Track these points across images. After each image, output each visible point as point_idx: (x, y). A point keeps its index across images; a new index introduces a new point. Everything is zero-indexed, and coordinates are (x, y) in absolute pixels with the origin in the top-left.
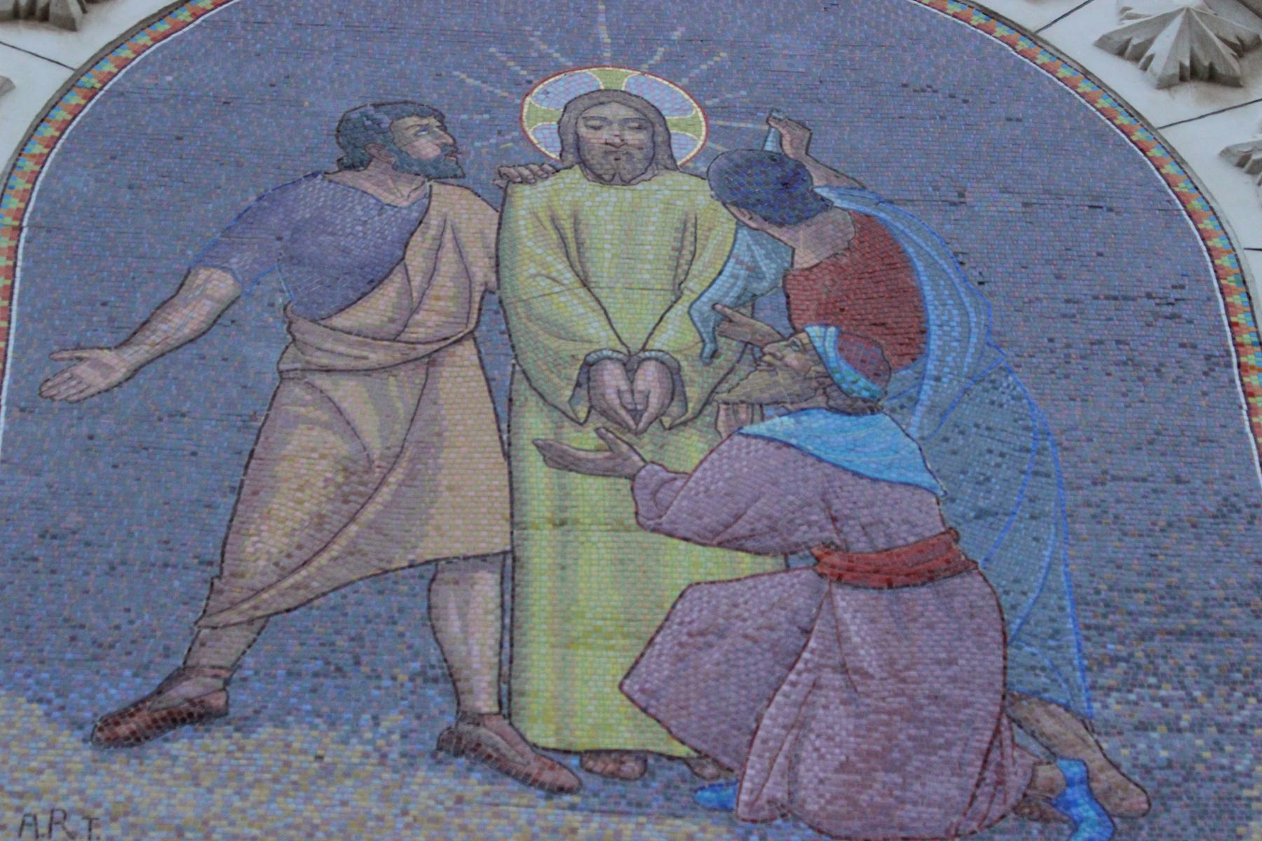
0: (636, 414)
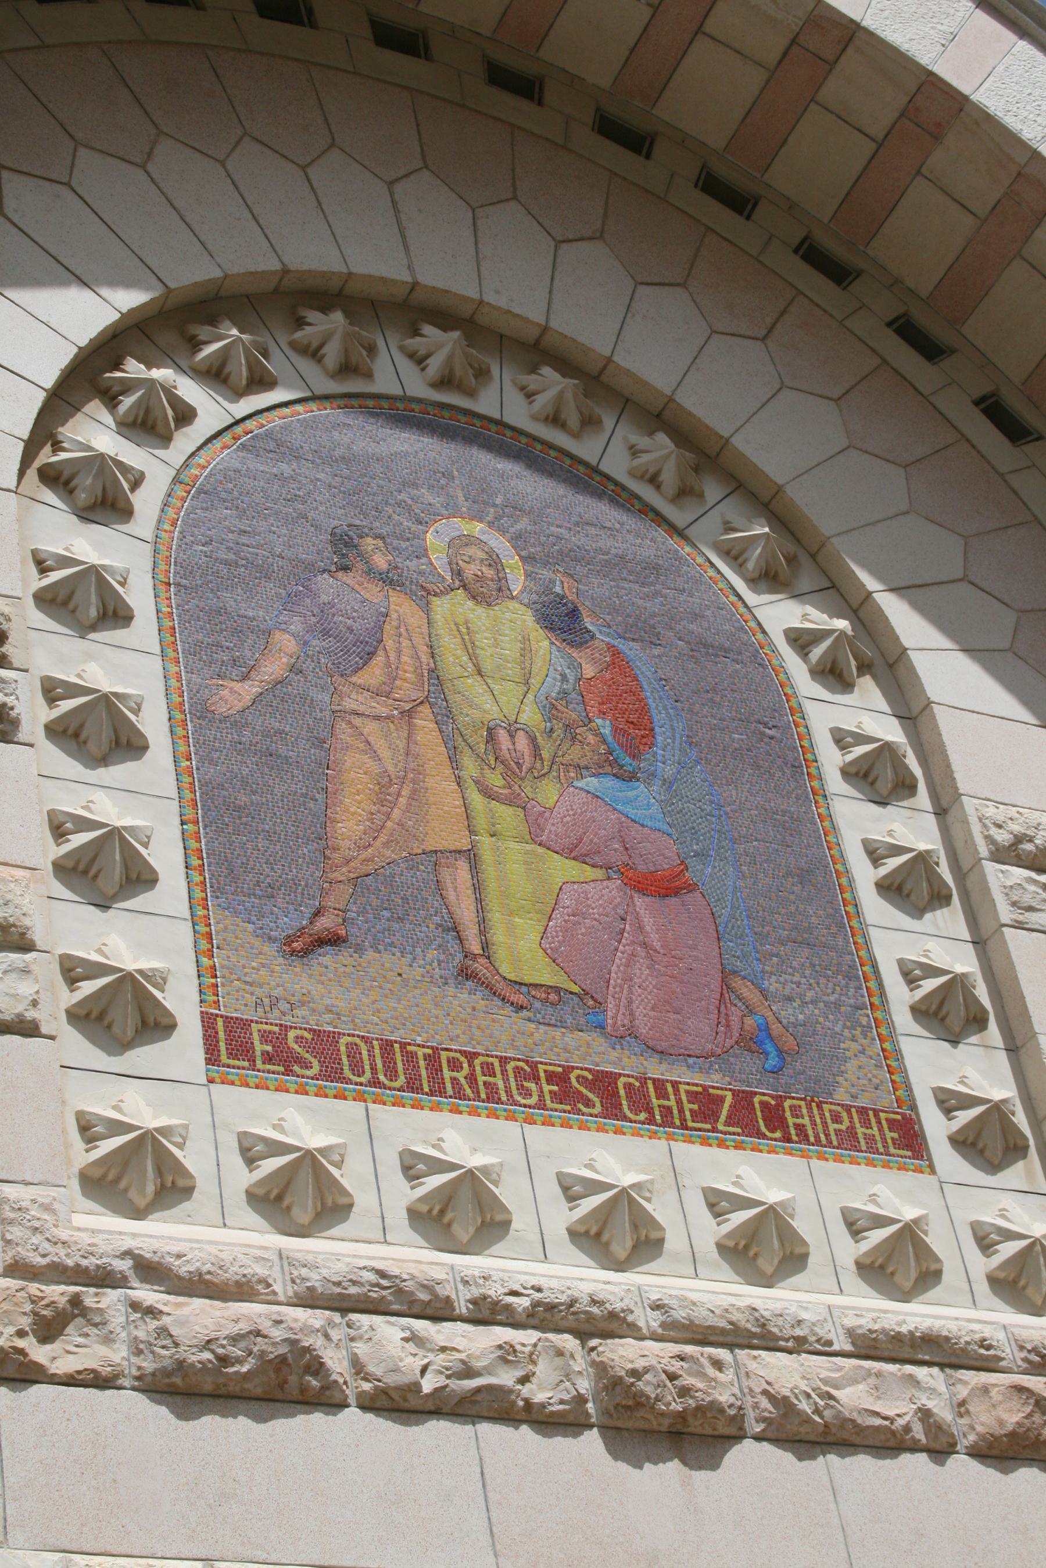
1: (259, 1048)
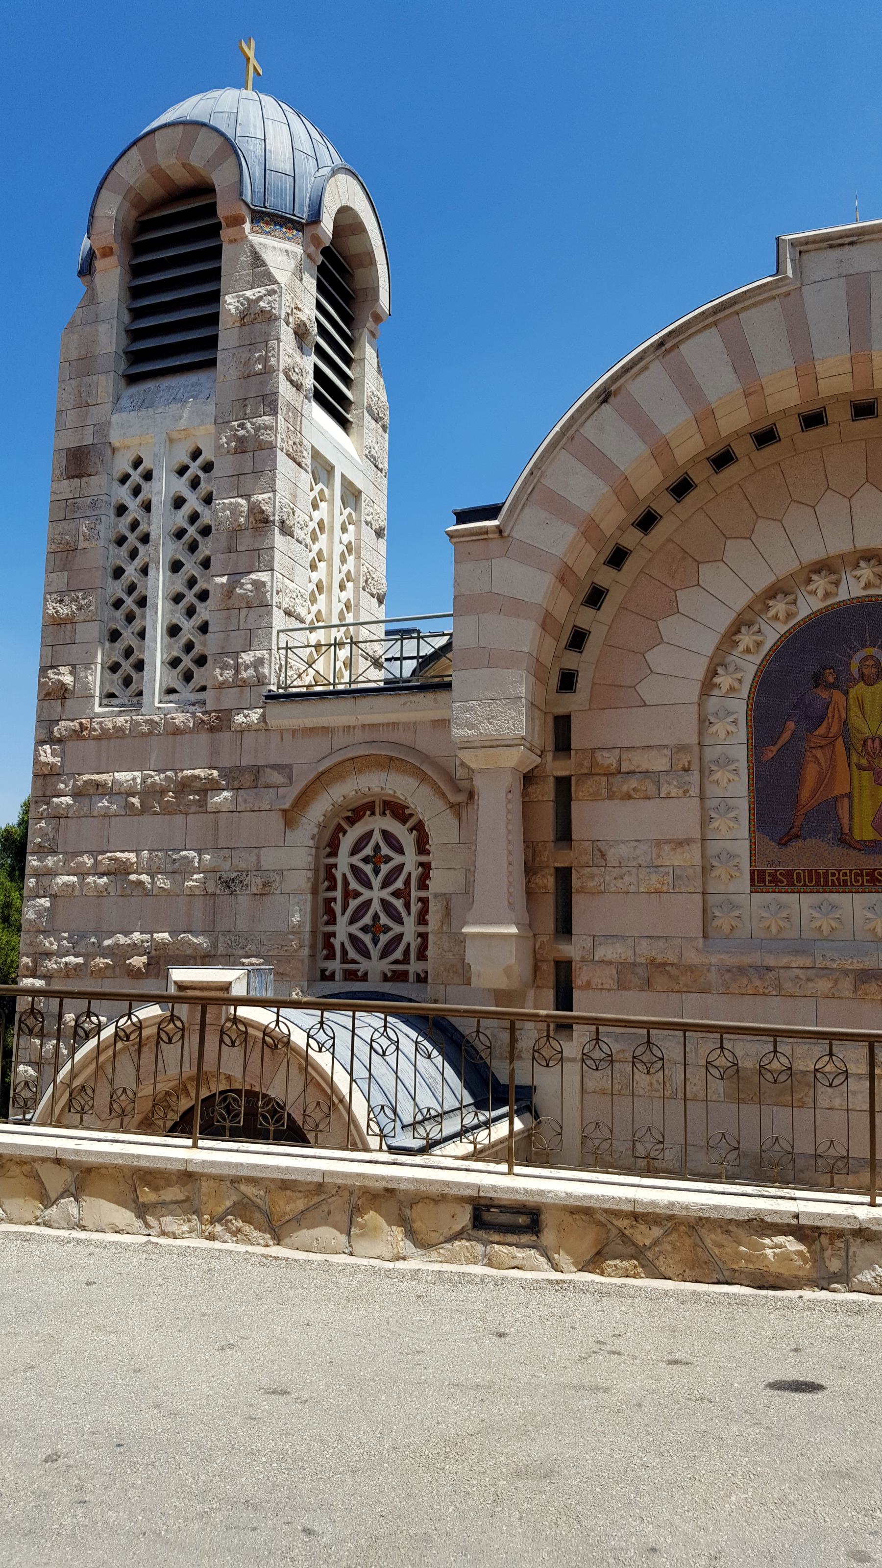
0: (874, 754)
1: (767, 878)
